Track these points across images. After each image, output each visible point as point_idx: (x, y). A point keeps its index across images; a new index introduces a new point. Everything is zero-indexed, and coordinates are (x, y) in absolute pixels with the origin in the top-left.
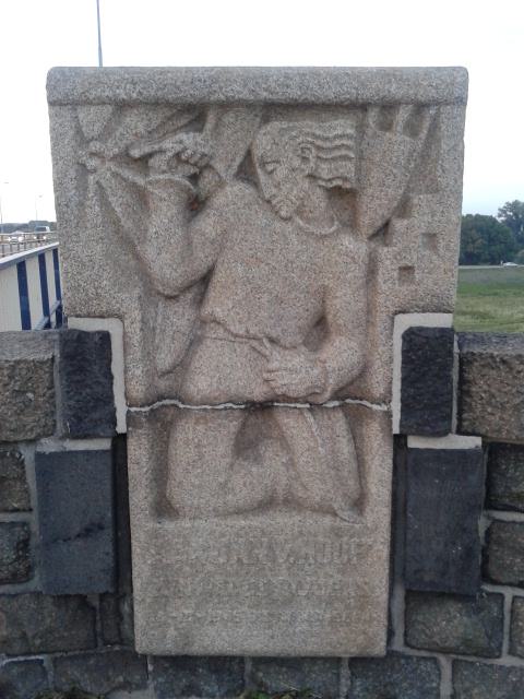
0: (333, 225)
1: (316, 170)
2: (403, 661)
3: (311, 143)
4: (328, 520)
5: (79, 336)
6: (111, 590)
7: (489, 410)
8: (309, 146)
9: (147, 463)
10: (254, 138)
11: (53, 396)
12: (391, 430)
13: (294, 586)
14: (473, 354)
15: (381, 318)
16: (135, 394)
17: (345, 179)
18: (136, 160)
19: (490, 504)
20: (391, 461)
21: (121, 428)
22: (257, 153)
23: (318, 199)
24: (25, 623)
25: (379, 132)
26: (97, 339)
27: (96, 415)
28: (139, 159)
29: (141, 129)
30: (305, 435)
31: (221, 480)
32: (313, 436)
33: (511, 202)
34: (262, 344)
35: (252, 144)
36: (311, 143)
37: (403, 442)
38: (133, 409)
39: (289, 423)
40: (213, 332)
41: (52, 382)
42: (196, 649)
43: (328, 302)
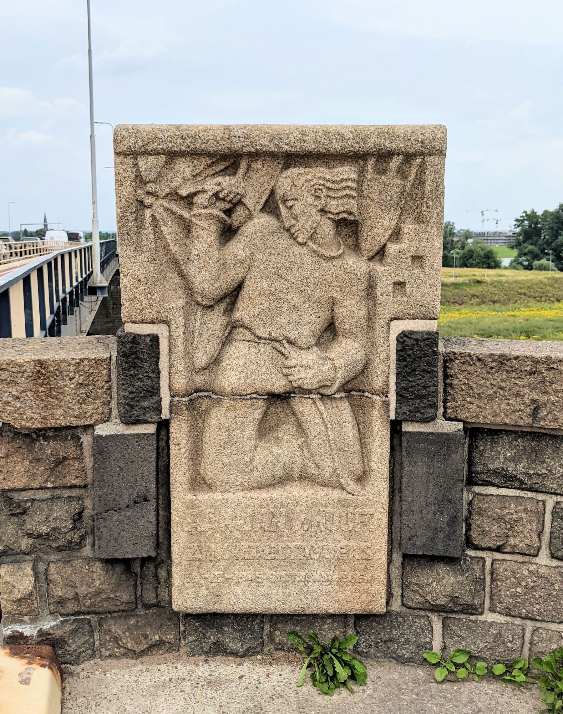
0: (339, 249)
1: (326, 206)
2: (400, 619)
3: (323, 185)
4: (336, 494)
5: (134, 337)
6: (153, 554)
7: (468, 399)
8: (321, 187)
9: (187, 444)
10: (277, 181)
11: (110, 388)
12: (389, 416)
13: (308, 551)
14: (454, 353)
15: (381, 322)
16: (177, 386)
17: (350, 213)
18: (183, 198)
19: (471, 482)
20: (388, 443)
21: (165, 414)
22: (279, 192)
23: (328, 228)
24: (78, 585)
25: (377, 176)
26: (148, 340)
27: (145, 404)
28: (186, 197)
29: (188, 174)
30: (317, 421)
31: (247, 459)
32: (324, 422)
33: (470, 231)
34: (283, 345)
35: (275, 185)
36: (323, 185)
37: (398, 428)
38: (176, 399)
39: (303, 411)
40: (240, 334)
41: (110, 377)
42: (223, 607)
43: (336, 311)
